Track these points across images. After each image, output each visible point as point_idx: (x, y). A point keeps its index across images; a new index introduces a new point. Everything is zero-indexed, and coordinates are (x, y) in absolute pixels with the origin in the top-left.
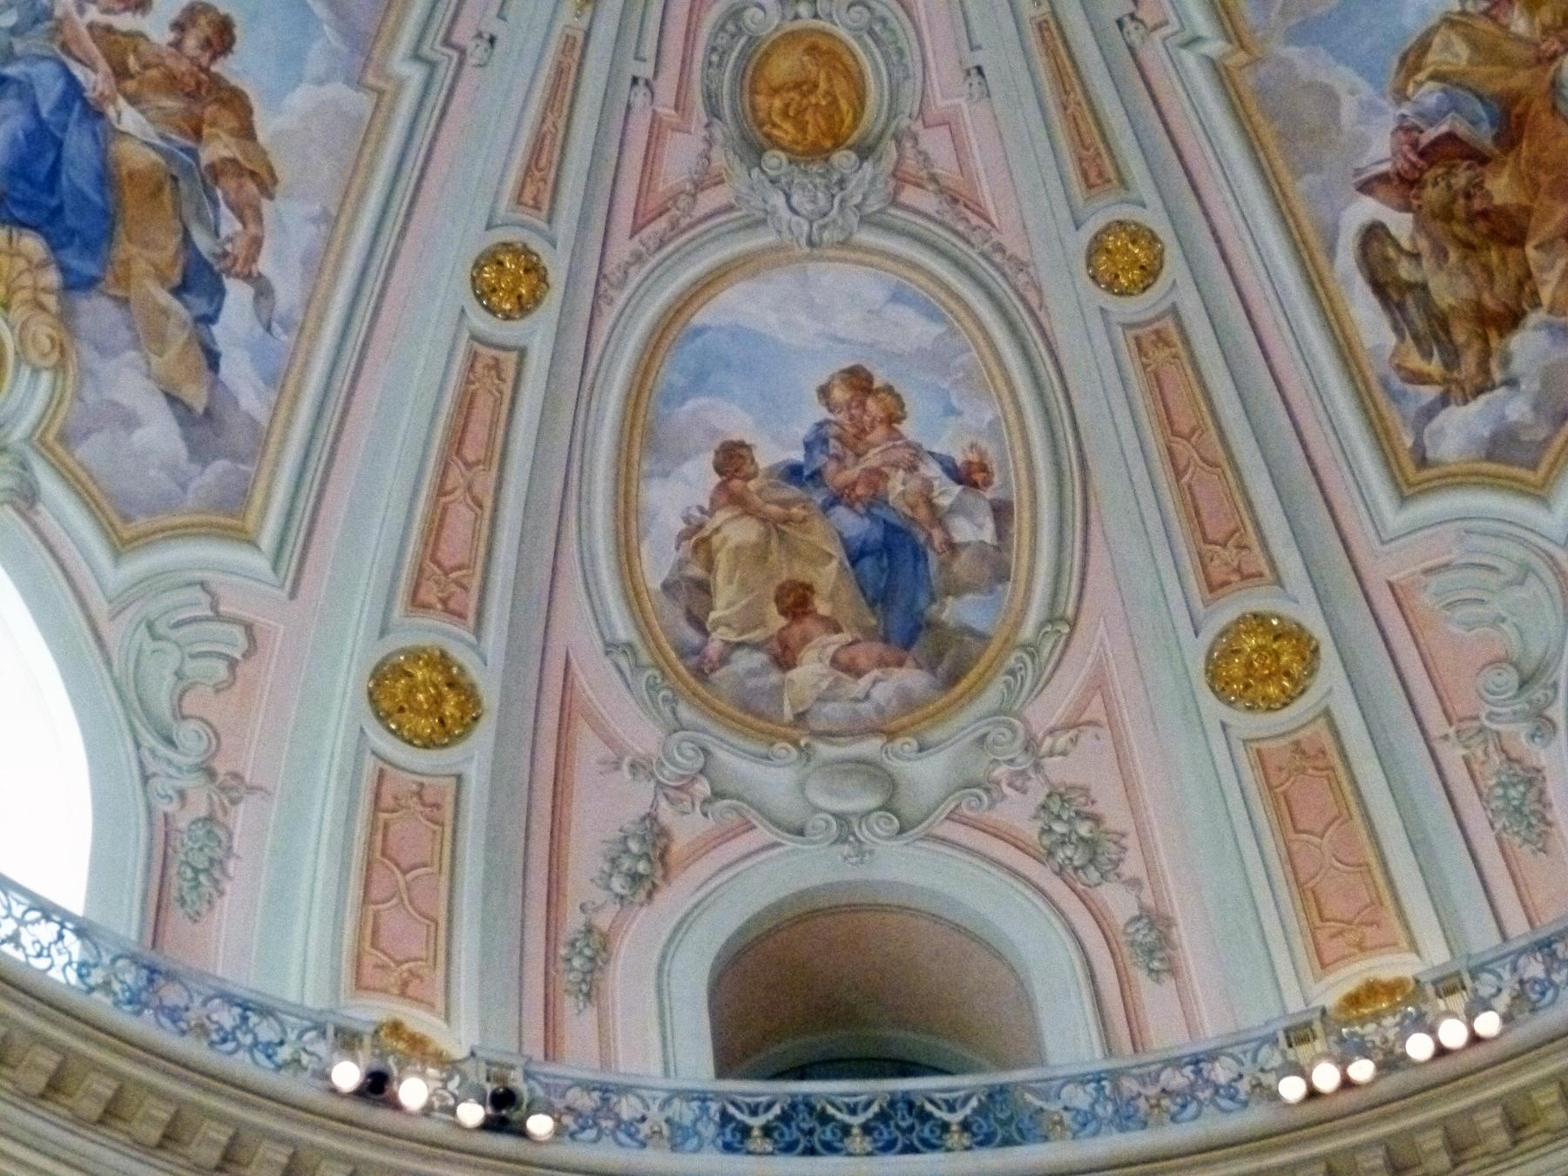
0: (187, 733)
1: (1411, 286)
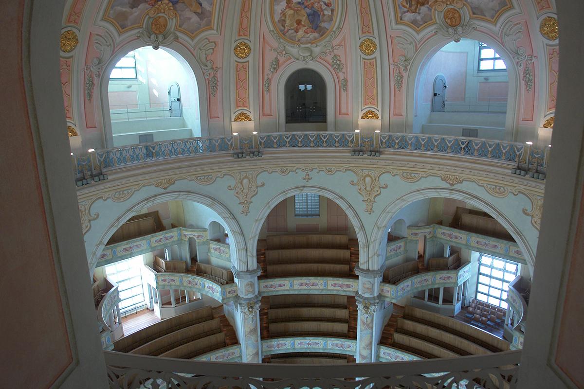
0: (209, 64)
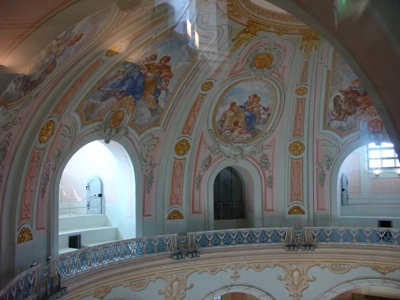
0: (148, 160)
1: (339, 104)
